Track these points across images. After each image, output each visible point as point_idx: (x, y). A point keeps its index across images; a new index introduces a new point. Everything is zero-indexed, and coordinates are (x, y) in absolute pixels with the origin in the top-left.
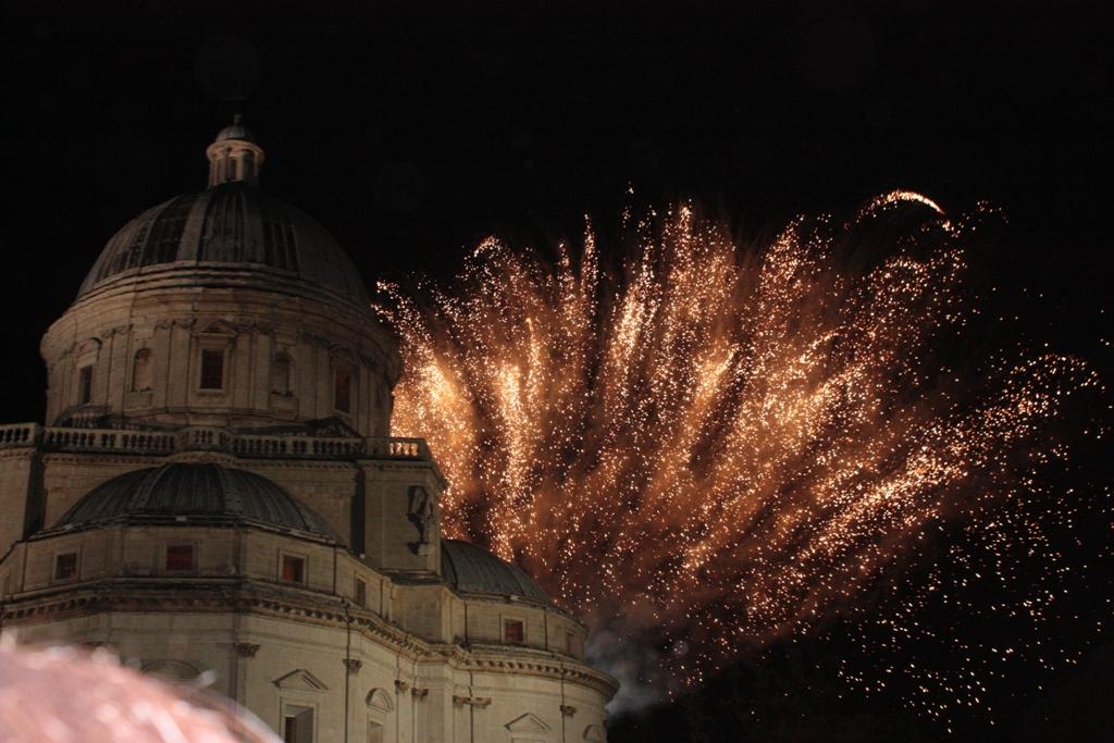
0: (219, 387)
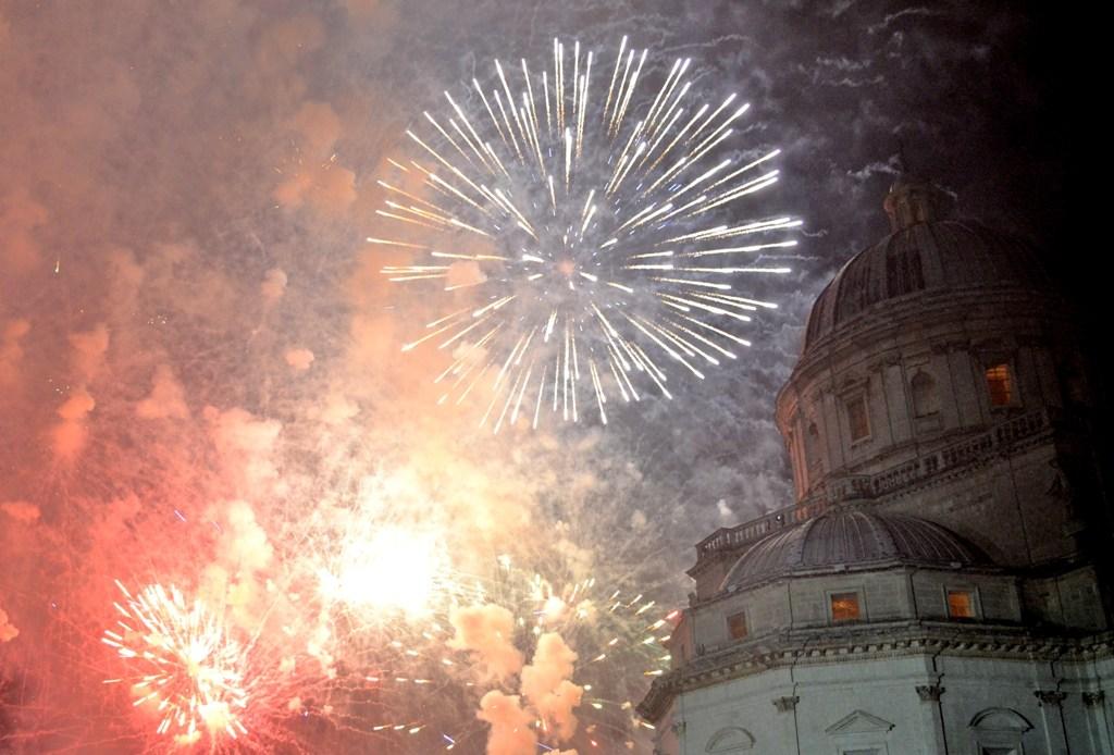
0: (866, 433)
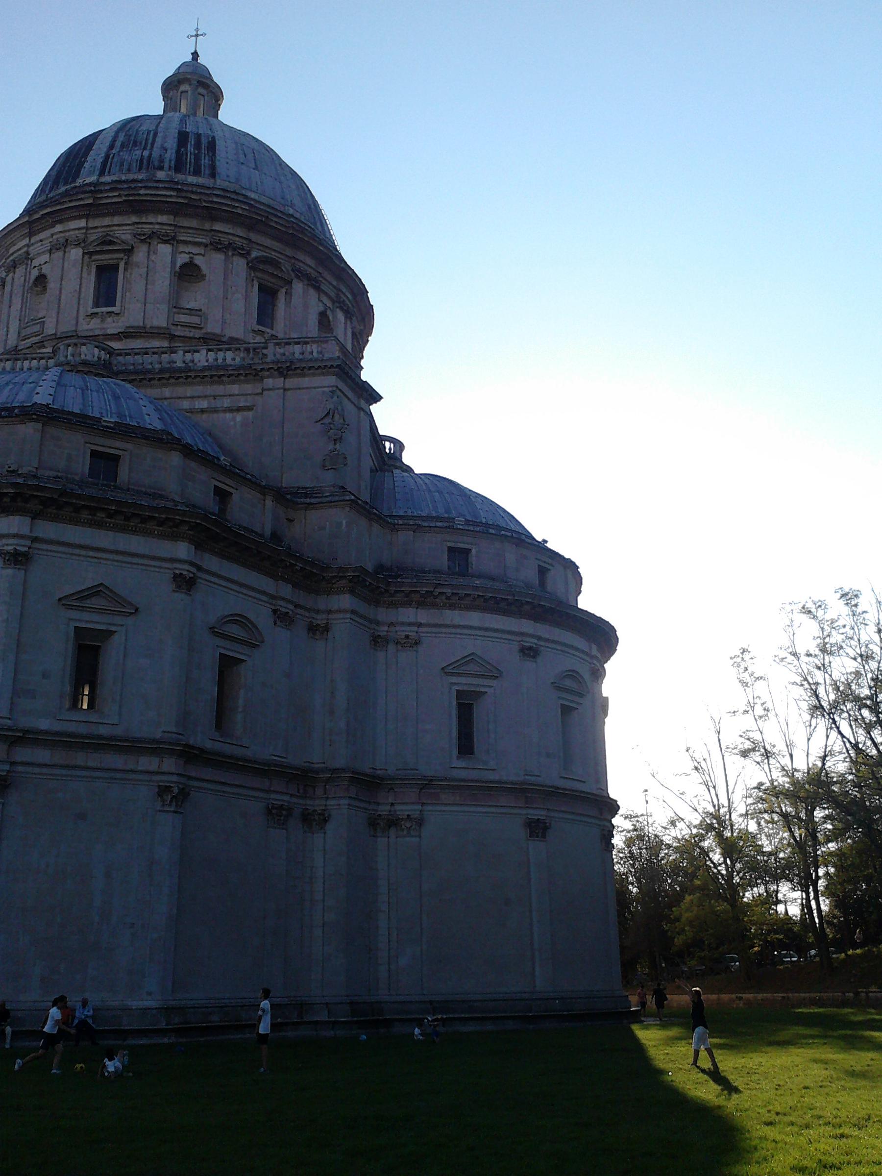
0: (114, 305)
